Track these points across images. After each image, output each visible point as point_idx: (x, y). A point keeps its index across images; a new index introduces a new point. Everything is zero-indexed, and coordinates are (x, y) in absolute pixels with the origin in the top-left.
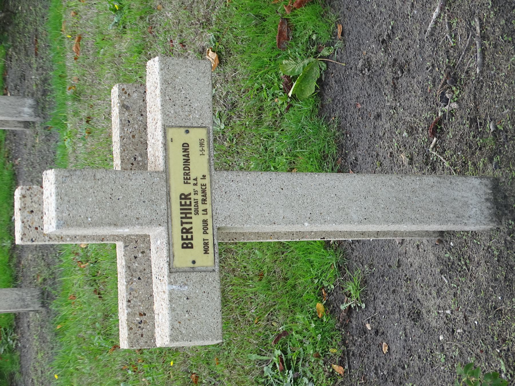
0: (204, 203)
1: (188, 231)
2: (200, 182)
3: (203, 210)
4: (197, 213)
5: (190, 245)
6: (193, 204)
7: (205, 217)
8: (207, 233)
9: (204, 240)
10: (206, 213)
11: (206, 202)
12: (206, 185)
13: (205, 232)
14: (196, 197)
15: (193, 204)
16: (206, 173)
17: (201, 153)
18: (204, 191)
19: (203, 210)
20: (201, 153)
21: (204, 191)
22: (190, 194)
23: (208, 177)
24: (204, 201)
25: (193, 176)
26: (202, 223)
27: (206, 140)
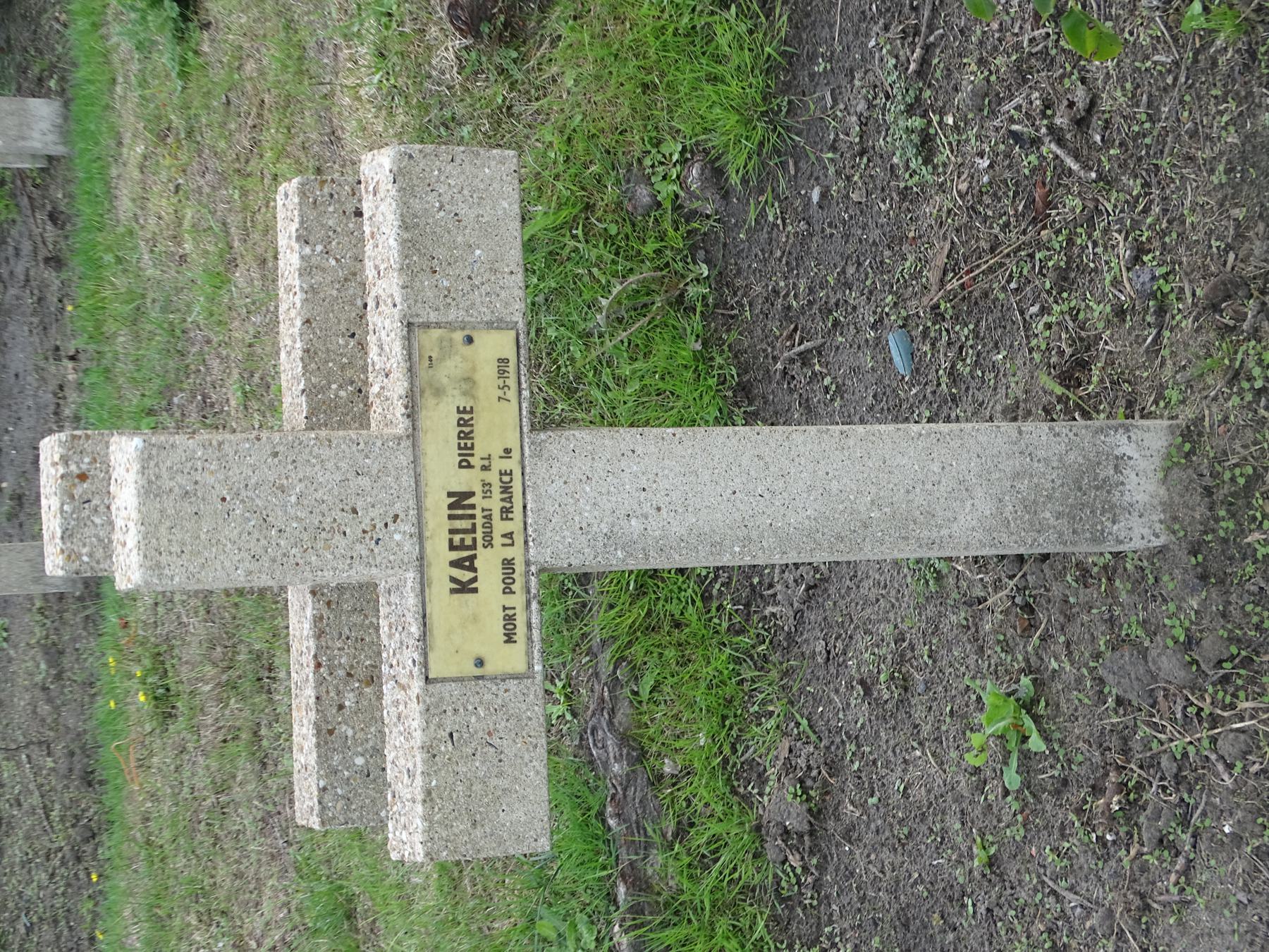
0: (507, 519)
2: (498, 465)
3: (504, 536)
4: (489, 544)
6: (479, 521)
7: (509, 553)
9: (505, 608)
10: (509, 541)
11: (510, 516)
12: (511, 474)
13: (508, 591)
16: (513, 443)
18: (506, 489)
19: (504, 536)
20: (500, 393)
21: (506, 489)
22: (472, 494)
23: (516, 454)
24: (506, 513)
25: (479, 451)
26: (500, 566)
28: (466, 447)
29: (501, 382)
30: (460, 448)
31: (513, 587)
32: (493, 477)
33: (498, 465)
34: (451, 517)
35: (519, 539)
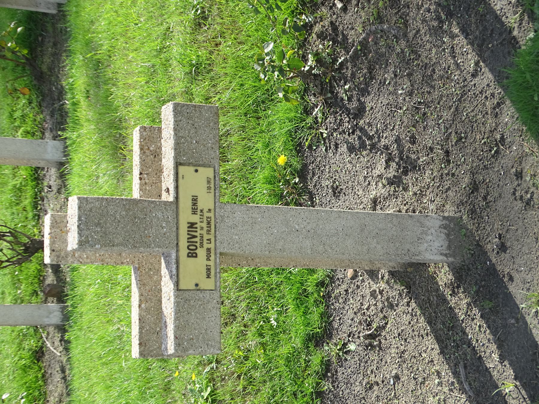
0: (209, 234)
2: (206, 214)
3: (207, 240)
7: (209, 246)
8: (210, 260)
9: (207, 266)
13: (208, 259)
16: (212, 207)
18: (209, 223)
19: (207, 240)
21: (209, 223)
23: (212, 211)
24: (209, 232)
28: (195, 209)
29: (208, 185)
30: (192, 209)
31: (210, 258)
35: (213, 240)
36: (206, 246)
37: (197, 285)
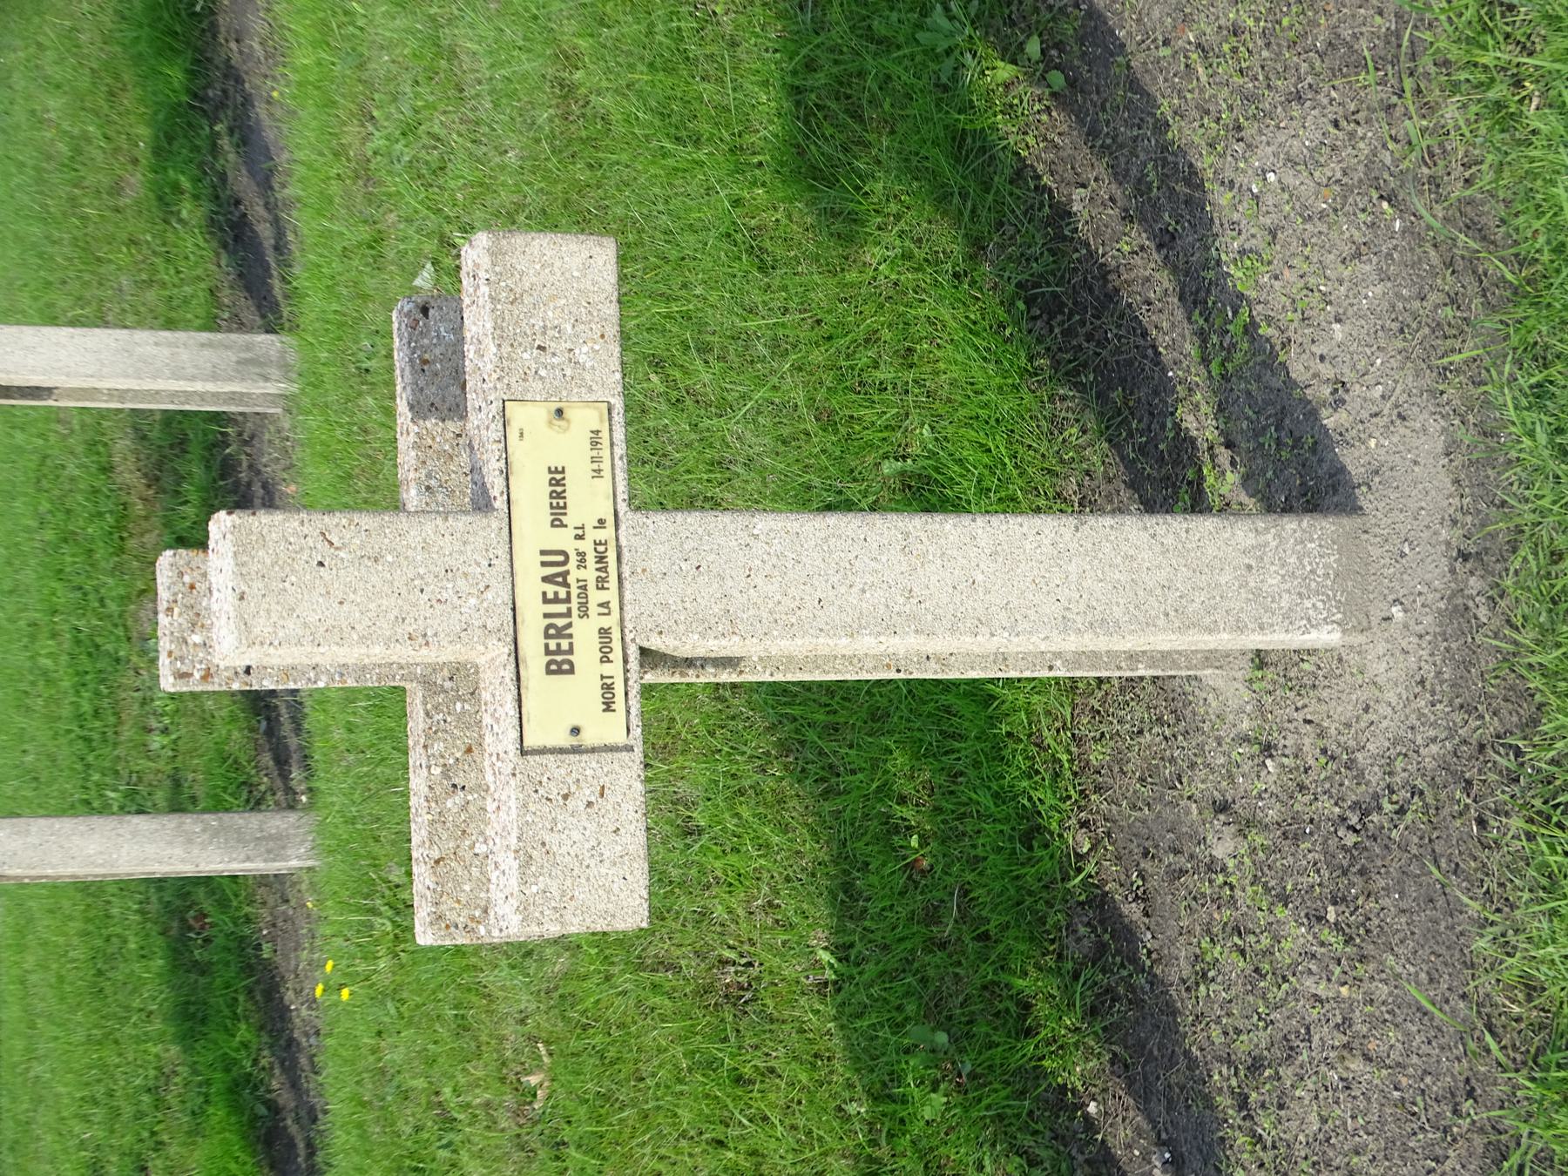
0: (603, 588)
1: (560, 633)
2: (592, 535)
3: (601, 605)
4: (584, 614)
5: (566, 667)
7: (605, 622)
8: (609, 661)
9: (602, 677)
13: (605, 659)
14: (582, 574)
15: (575, 592)
17: (595, 466)
18: (601, 559)
19: (601, 605)
20: (595, 466)
21: (601, 559)
24: (601, 584)
27: (605, 435)
29: (594, 453)
32: (587, 546)
33: (592, 535)
34: (544, 564)
36: (596, 621)
37: (576, 731)
